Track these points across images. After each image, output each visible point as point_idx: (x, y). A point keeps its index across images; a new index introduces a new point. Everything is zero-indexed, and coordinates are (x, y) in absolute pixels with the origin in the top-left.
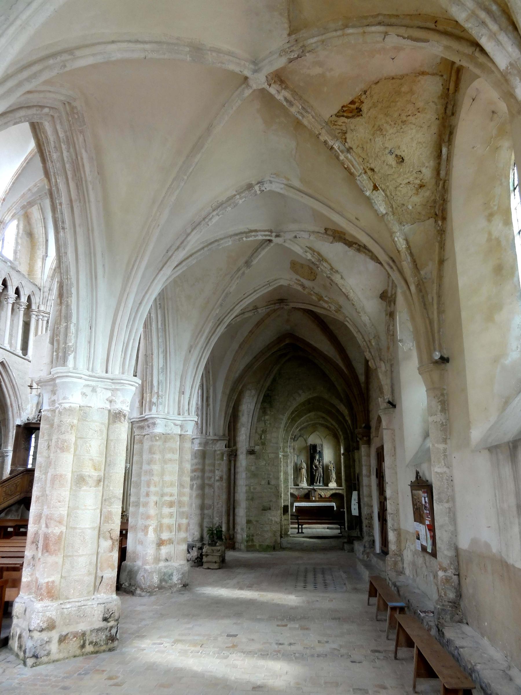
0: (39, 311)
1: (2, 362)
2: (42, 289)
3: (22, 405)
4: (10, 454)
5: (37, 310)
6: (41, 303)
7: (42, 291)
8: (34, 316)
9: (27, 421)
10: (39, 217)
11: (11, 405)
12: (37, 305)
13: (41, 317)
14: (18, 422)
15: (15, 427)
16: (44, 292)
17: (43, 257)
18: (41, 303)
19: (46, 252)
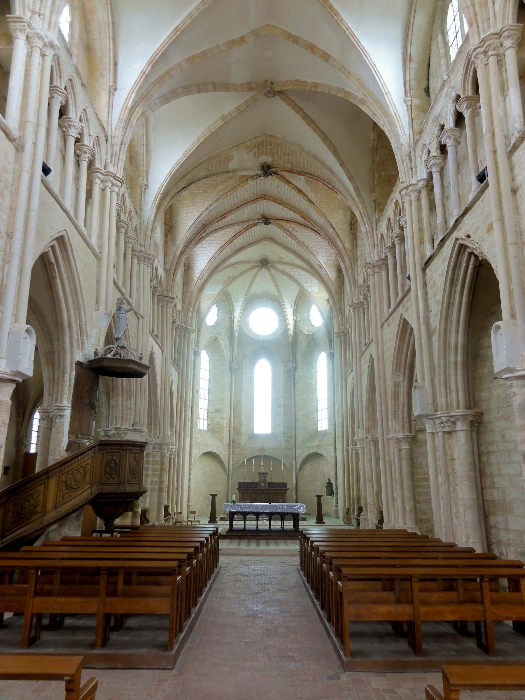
0: (108, 174)
1: (62, 237)
2: (109, 138)
3: (86, 327)
4: (68, 413)
5: (103, 171)
6: (109, 161)
7: (109, 142)
8: (98, 181)
9: (92, 358)
10: (106, 20)
11: (70, 323)
12: (103, 163)
13: (110, 185)
14: (79, 357)
15: (74, 366)
16: (112, 145)
17: (110, 89)
18: (109, 161)
19: (115, 82)
